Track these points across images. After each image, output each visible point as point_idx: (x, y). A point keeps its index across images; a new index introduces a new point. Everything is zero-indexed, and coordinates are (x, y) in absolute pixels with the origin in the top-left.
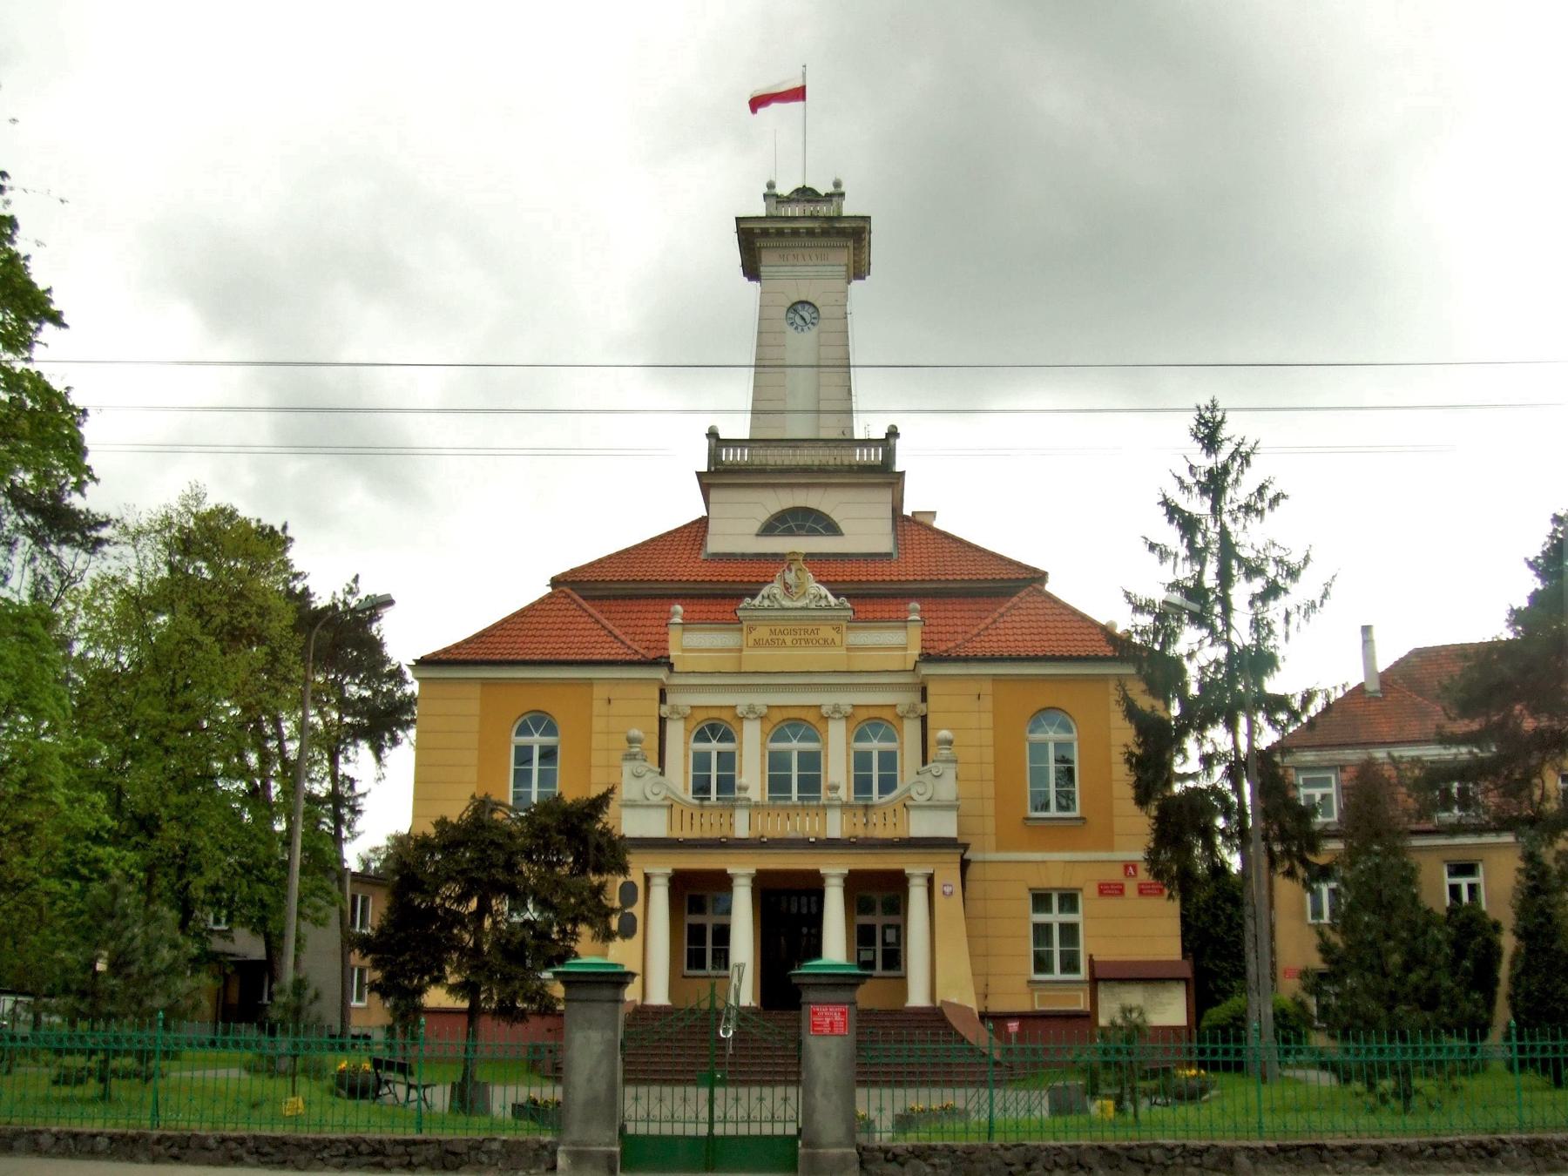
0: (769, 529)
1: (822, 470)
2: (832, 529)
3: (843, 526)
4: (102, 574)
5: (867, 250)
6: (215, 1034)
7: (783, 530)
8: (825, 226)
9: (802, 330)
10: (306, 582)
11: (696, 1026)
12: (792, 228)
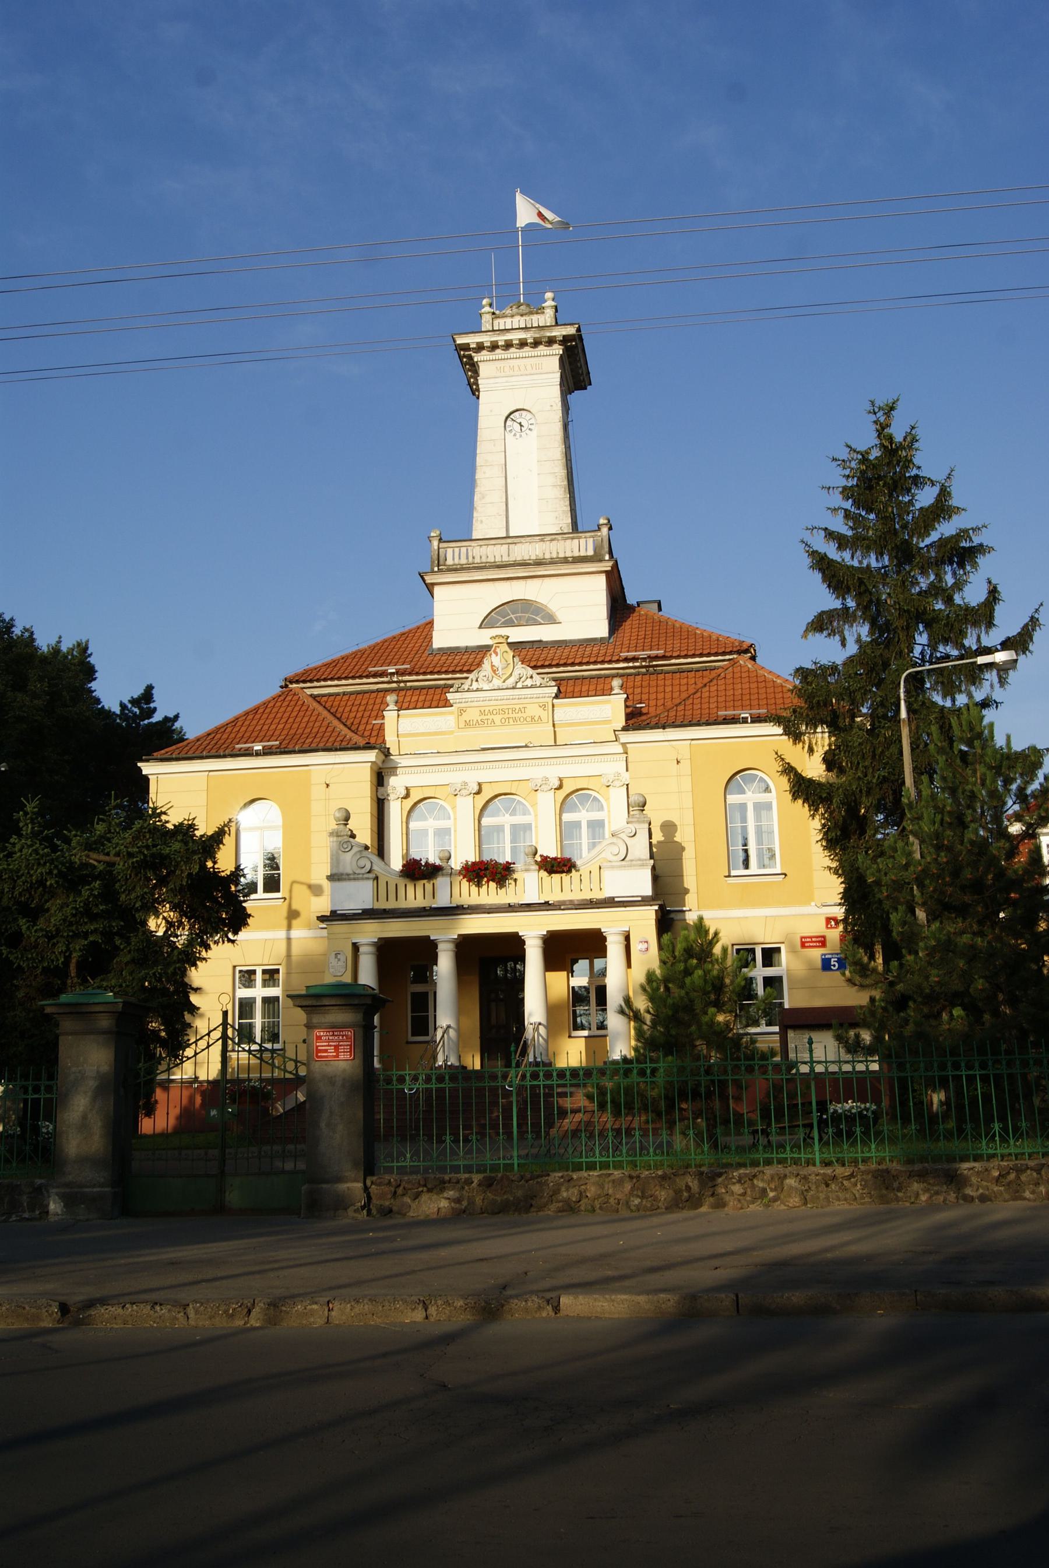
0: (486, 623)
1: (539, 563)
2: (551, 619)
3: (559, 617)
4: (925, 778)
5: (581, 355)
6: (798, 1126)
7: (503, 623)
8: (537, 336)
9: (521, 436)
10: (126, 702)
11: (572, 1085)
12: (506, 341)
